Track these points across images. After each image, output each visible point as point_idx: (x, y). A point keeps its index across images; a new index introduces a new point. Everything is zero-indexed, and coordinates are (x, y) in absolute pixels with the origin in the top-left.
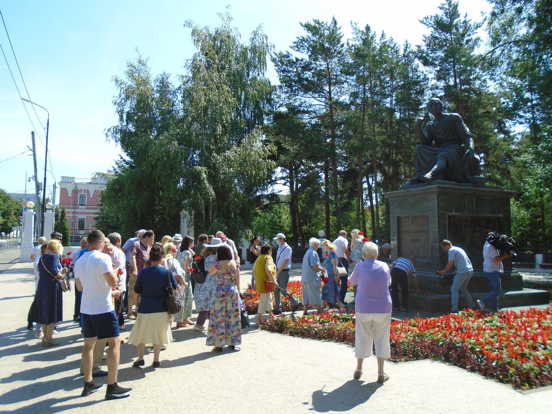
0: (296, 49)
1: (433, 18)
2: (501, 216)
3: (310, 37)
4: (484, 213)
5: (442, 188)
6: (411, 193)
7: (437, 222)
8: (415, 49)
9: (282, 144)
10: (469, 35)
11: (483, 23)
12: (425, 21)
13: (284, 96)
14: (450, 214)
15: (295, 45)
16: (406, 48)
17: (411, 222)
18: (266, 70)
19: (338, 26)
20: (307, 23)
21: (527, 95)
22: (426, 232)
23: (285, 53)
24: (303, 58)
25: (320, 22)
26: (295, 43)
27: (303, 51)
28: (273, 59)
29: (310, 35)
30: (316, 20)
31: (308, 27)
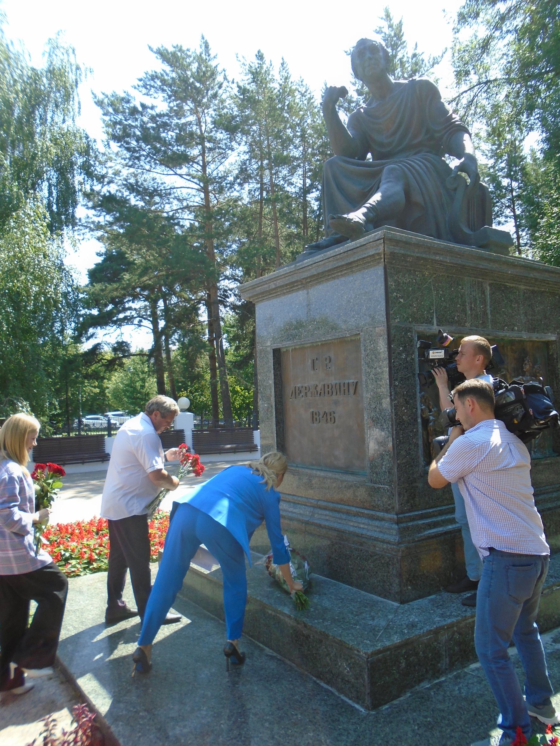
0: (144, 91)
3: (168, 72)
4: (513, 330)
9: (127, 255)
11: (442, 56)
13: (127, 172)
15: (141, 83)
17: (310, 362)
18: (79, 112)
19: (212, 53)
20: (160, 47)
21: (505, 182)
22: (352, 391)
23: (123, 95)
24: (154, 104)
25: (184, 48)
26: (140, 80)
27: (155, 95)
28: (98, 101)
29: (168, 69)
30: (177, 46)
31: (164, 55)
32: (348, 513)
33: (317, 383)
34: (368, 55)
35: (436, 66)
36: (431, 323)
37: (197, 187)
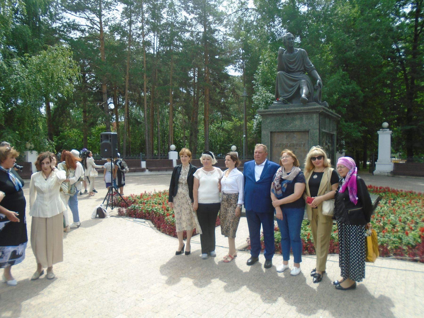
22: (302, 146)
33: (288, 142)
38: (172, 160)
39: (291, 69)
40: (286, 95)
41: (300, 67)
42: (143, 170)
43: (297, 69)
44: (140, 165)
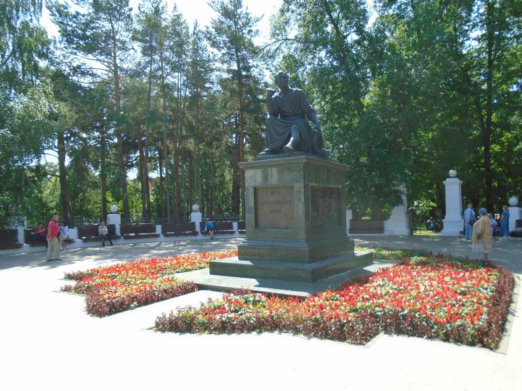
1: (220, 3)
2: (340, 187)
5: (308, 159)
6: (273, 163)
7: (303, 192)
8: (204, 29)
10: (250, 26)
12: (212, 5)
13: (60, 53)
14: (311, 184)
16: (196, 26)
18: (41, 15)
22: (288, 203)
27: (83, 6)
32: (288, 242)
34: (283, 80)
35: (258, 22)
36: (313, 182)
37: (106, 68)
38: (194, 223)
39: (286, 112)
40: (276, 144)
41: (295, 111)
42: (157, 236)
43: (293, 112)
44: (154, 230)
